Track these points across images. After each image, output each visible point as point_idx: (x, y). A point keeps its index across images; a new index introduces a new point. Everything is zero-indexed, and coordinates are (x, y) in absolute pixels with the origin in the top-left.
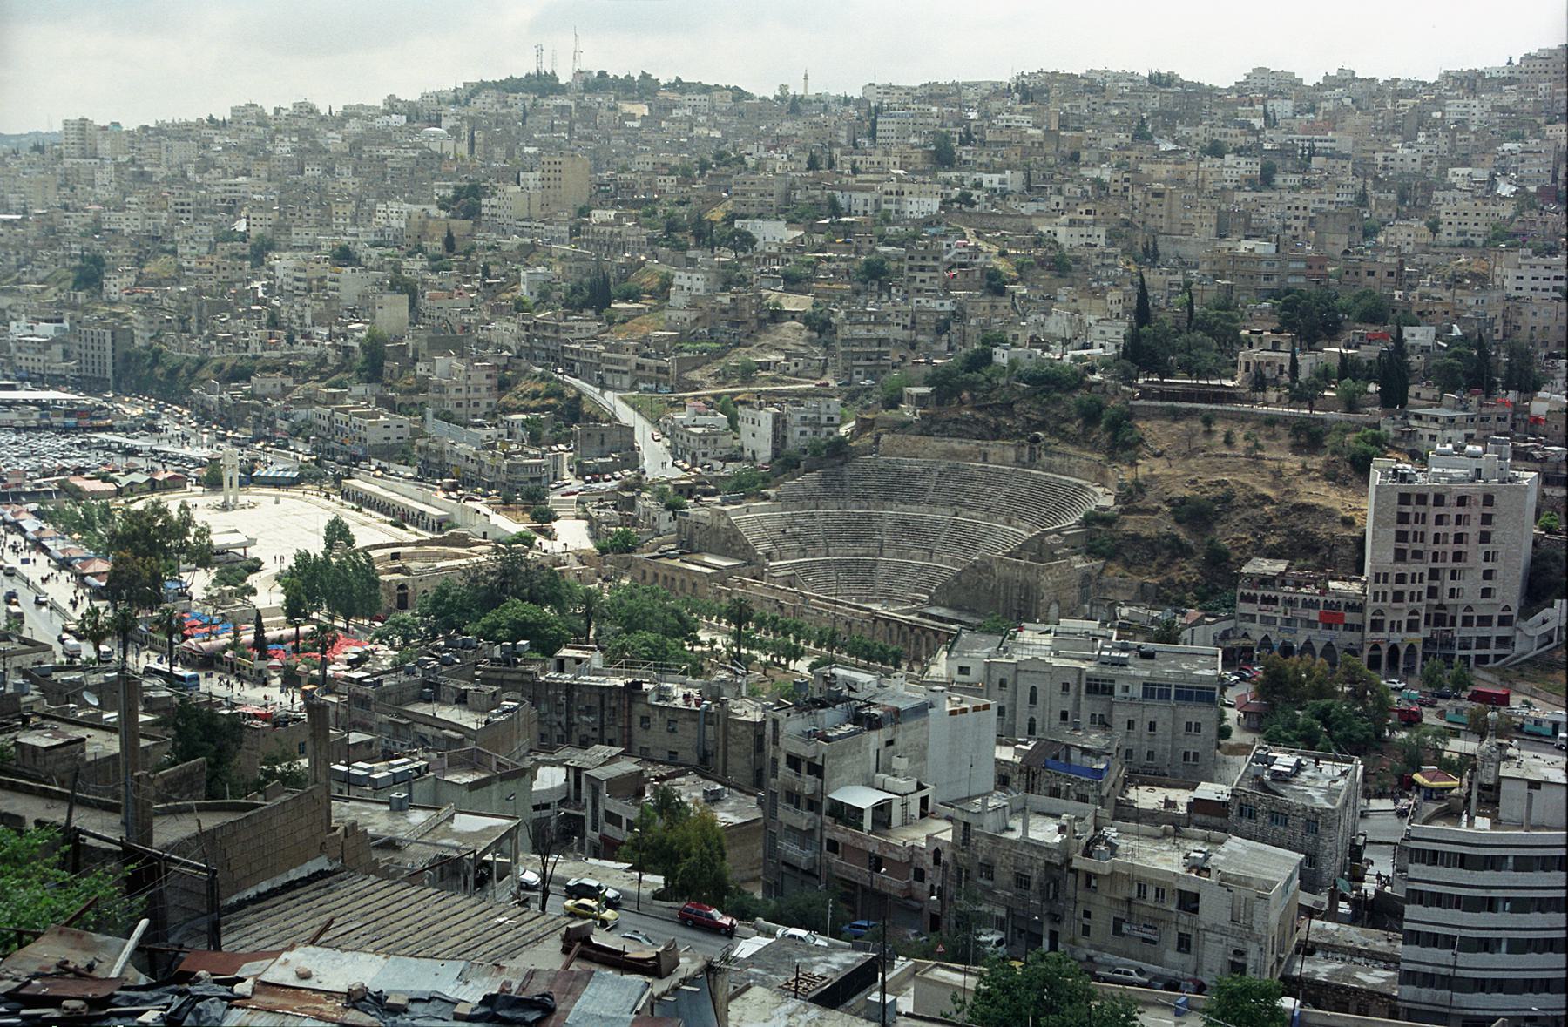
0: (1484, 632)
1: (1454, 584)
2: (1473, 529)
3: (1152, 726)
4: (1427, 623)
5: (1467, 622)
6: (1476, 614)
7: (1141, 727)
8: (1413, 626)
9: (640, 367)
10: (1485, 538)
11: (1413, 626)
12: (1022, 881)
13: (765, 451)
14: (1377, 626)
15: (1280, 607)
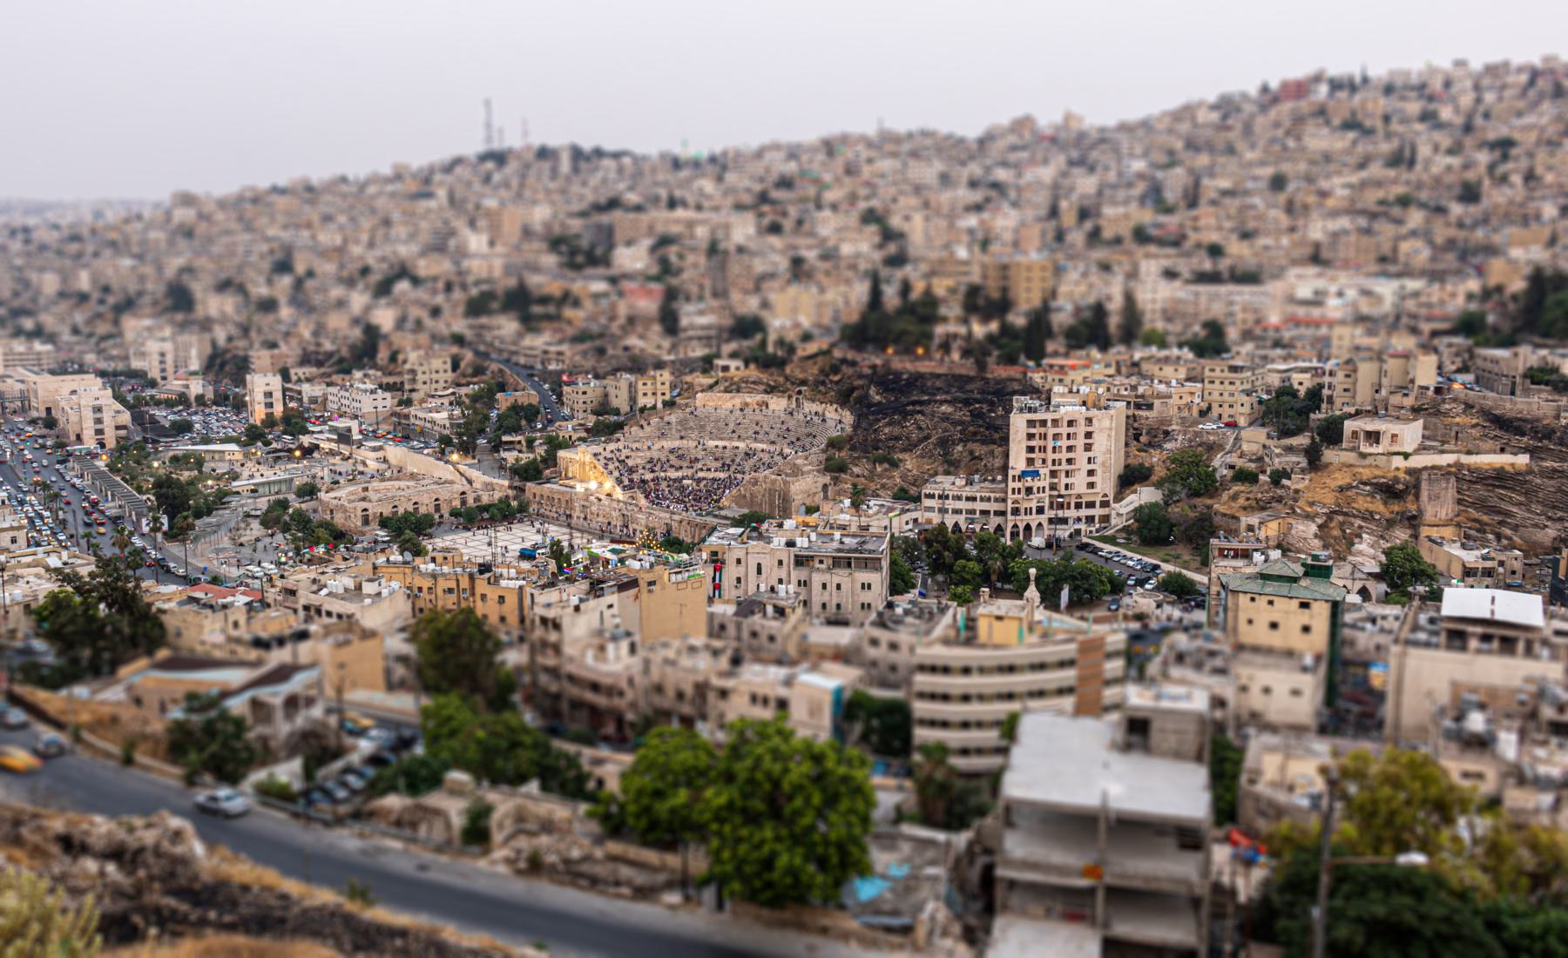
0: (1090, 512)
1: (1069, 481)
2: (1080, 442)
3: (839, 587)
4: (1051, 507)
5: (1078, 506)
6: (1084, 500)
7: (832, 587)
8: (1040, 511)
9: (546, 352)
10: (1088, 447)
11: (1040, 511)
12: (680, 696)
13: (625, 408)
14: (1016, 512)
15: (950, 501)
